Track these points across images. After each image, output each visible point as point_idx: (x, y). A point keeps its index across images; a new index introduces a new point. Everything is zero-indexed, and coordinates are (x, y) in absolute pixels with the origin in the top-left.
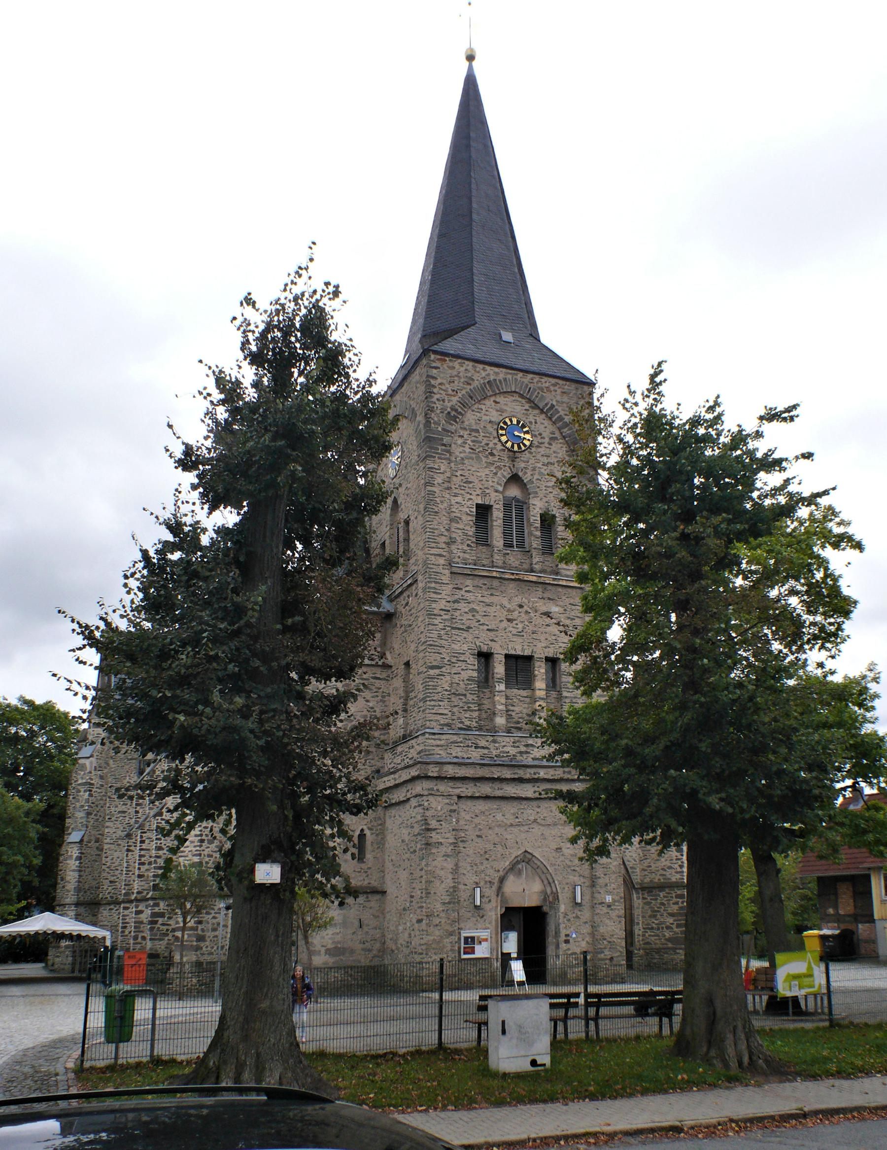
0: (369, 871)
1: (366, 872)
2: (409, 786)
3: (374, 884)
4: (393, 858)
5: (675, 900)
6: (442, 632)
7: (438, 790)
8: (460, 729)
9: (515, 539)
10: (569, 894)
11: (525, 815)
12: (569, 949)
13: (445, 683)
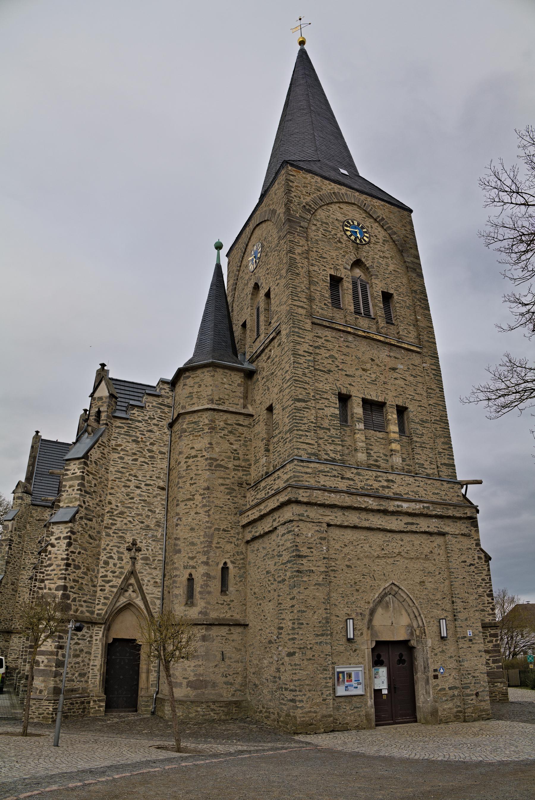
0: (232, 604)
1: (229, 605)
2: (276, 515)
3: (237, 617)
4: (256, 590)
5: (489, 639)
6: (306, 371)
7: (308, 516)
8: (326, 460)
9: (362, 310)
10: (435, 629)
11: (390, 547)
13: (310, 415)
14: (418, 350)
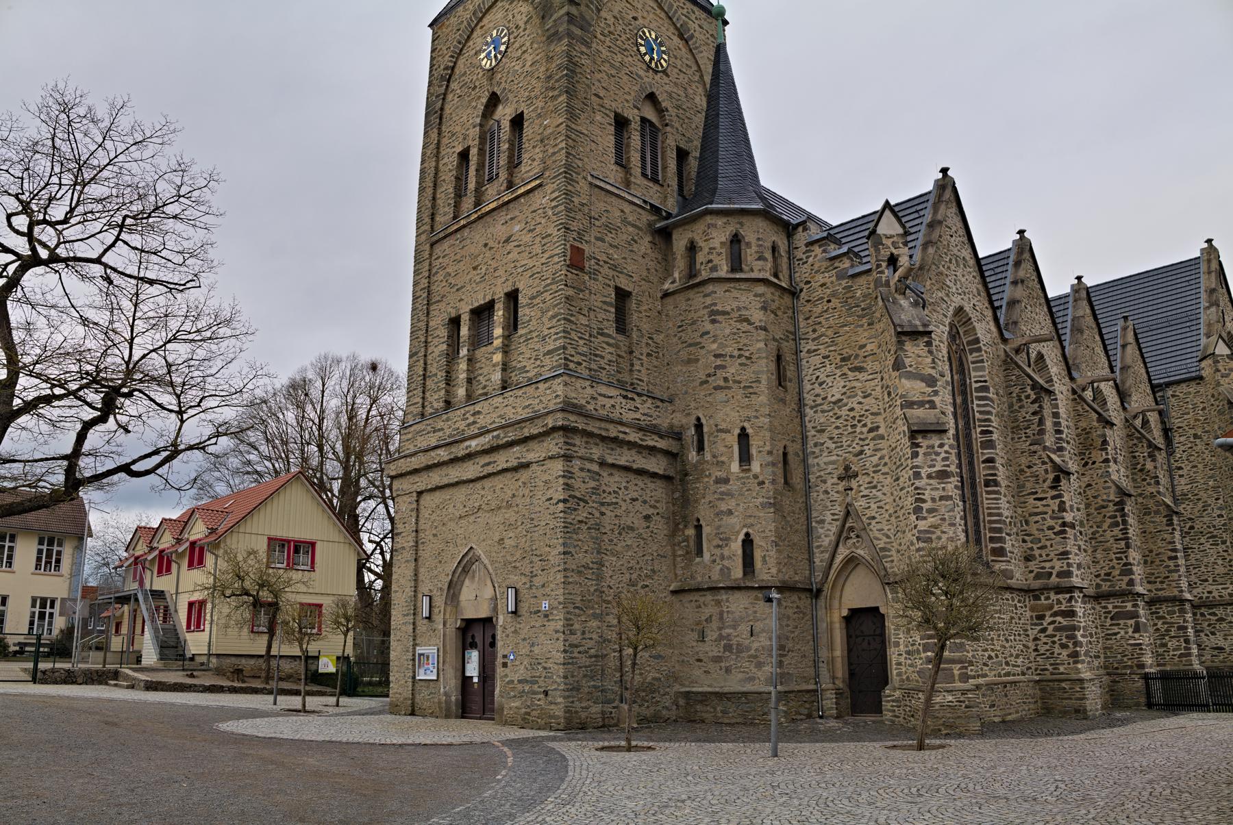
12: (506, 676)
14: (538, 182)
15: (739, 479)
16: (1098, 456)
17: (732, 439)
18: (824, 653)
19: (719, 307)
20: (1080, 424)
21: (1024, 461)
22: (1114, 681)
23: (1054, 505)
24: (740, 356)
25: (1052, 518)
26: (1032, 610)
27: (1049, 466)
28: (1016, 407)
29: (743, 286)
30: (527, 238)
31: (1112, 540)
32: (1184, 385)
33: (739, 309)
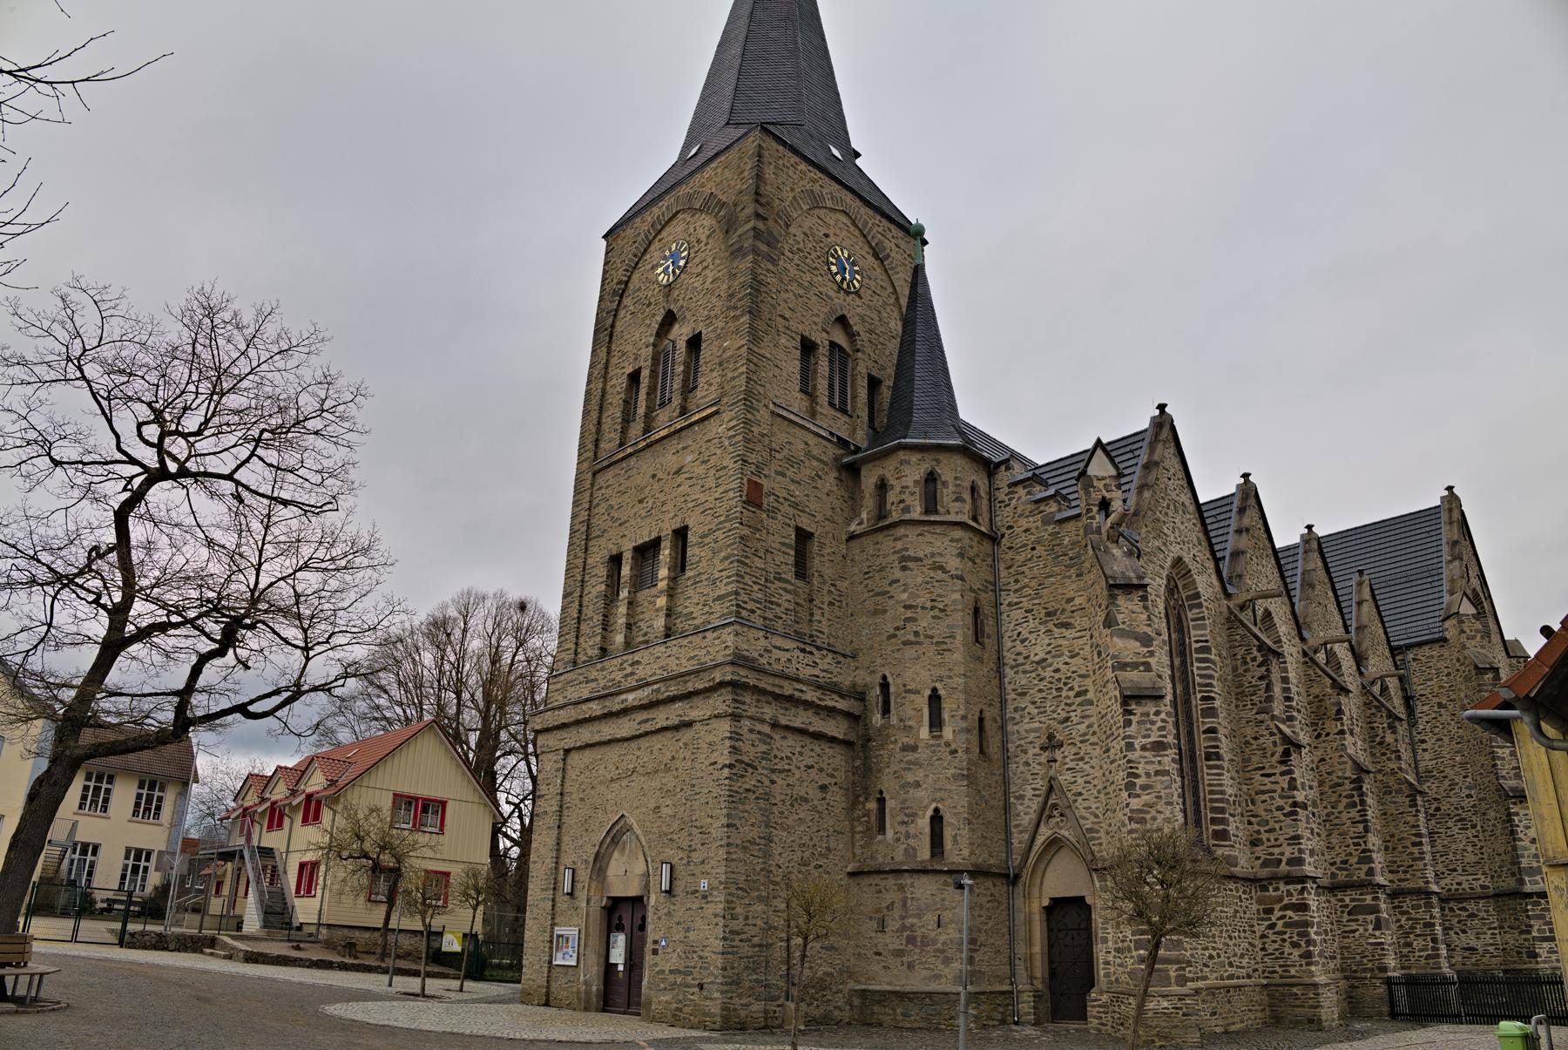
15: (928, 746)
16: (1333, 727)
17: (922, 702)
18: (1021, 949)
19: (911, 553)
20: (1312, 690)
21: (1250, 731)
22: (1352, 986)
23: (1284, 782)
24: (933, 608)
25: (1281, 797)
26: (1259, 902)
27: (1277, 738)
28: (1240, 671)
29: (939, 529)
30: (700, 470)
31: (1349, 823)
32: (1426, 648)
33: (933, 555)
